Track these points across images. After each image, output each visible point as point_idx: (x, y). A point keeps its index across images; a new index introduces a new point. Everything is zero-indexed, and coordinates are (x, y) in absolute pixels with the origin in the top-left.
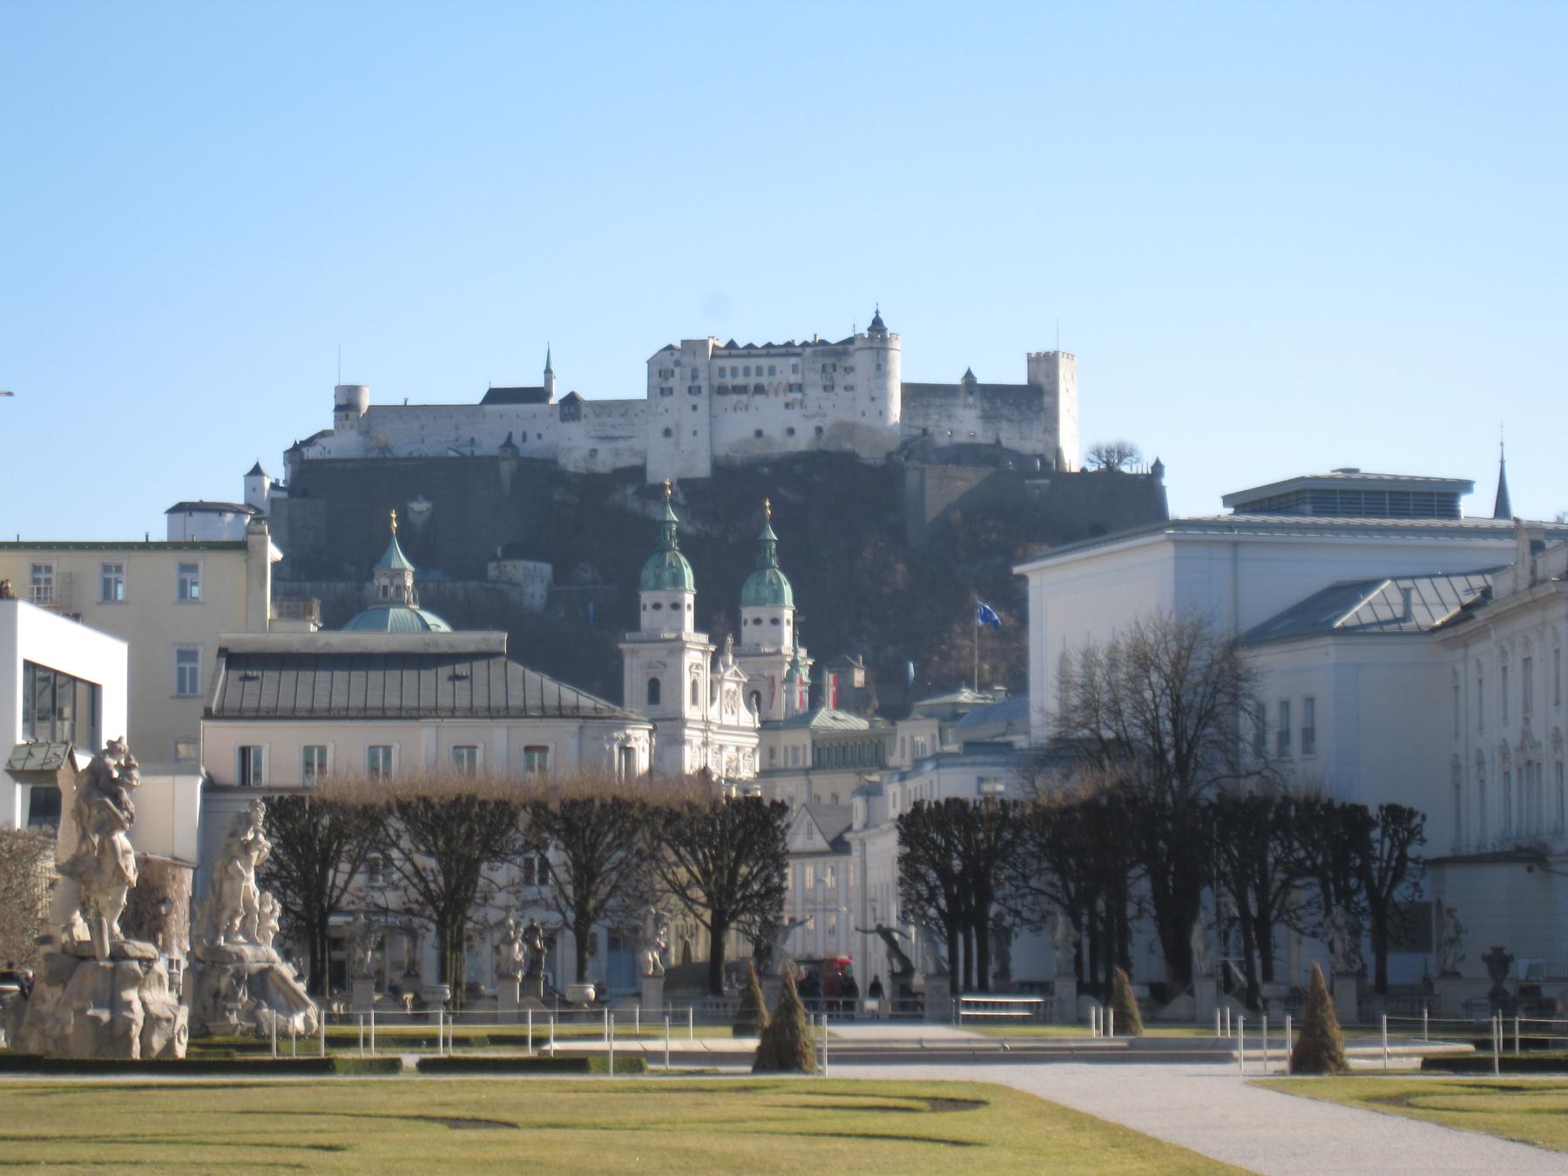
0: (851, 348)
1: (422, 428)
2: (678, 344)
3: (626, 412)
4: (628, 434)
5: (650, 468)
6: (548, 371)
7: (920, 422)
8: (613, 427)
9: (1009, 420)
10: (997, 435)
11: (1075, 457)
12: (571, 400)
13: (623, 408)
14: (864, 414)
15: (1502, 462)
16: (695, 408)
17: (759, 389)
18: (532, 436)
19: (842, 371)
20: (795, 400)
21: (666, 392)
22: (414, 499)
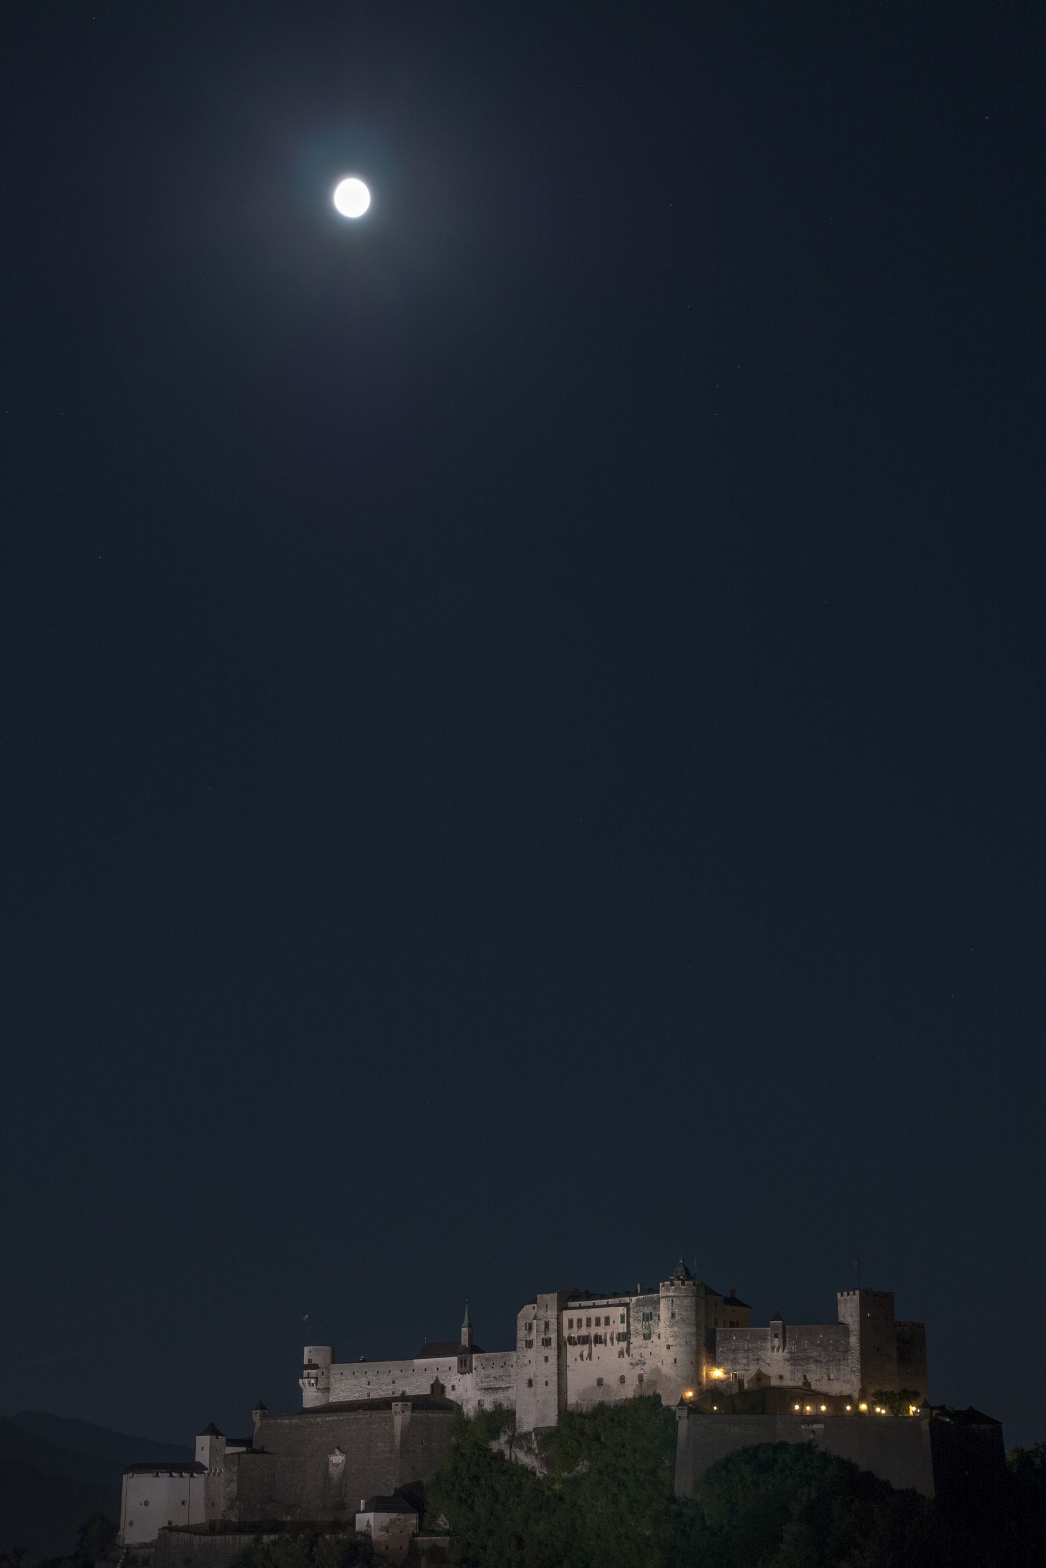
3: (505, 1363)
4: (508, 1385)
8: (495, 1378)
9: (816, 1361)
10: (805, 1377)
16: (546, 1359)
17: (598, 1340)
21: (529, 1344)
22: (333, 1453)
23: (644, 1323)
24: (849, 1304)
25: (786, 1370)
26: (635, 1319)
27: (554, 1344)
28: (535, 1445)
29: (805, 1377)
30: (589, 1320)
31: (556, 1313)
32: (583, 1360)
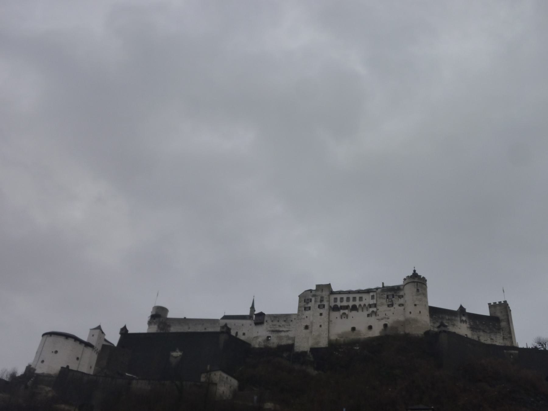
2: (314, 288)
4: (287, 330)
5: (296, 344)
6: (252, 308)
8: (280, 326)
9: (484, 331)
10: (478, 337)
12: (261, 314)
13: (286, 318)
14: (410, 313)
16: (321, 314)
17: (354, 308)
19: (397, 297)
20: (373, 312)
21: (307, 309)
22: (174, 350)
23: (388, 300)
24: (498, 308)
26: (380, 298)
27: (327, 307)
28: (311, 356)
29: (478, 337)
30: (348, 299)
31: (328, 293)
32: (341, 318)
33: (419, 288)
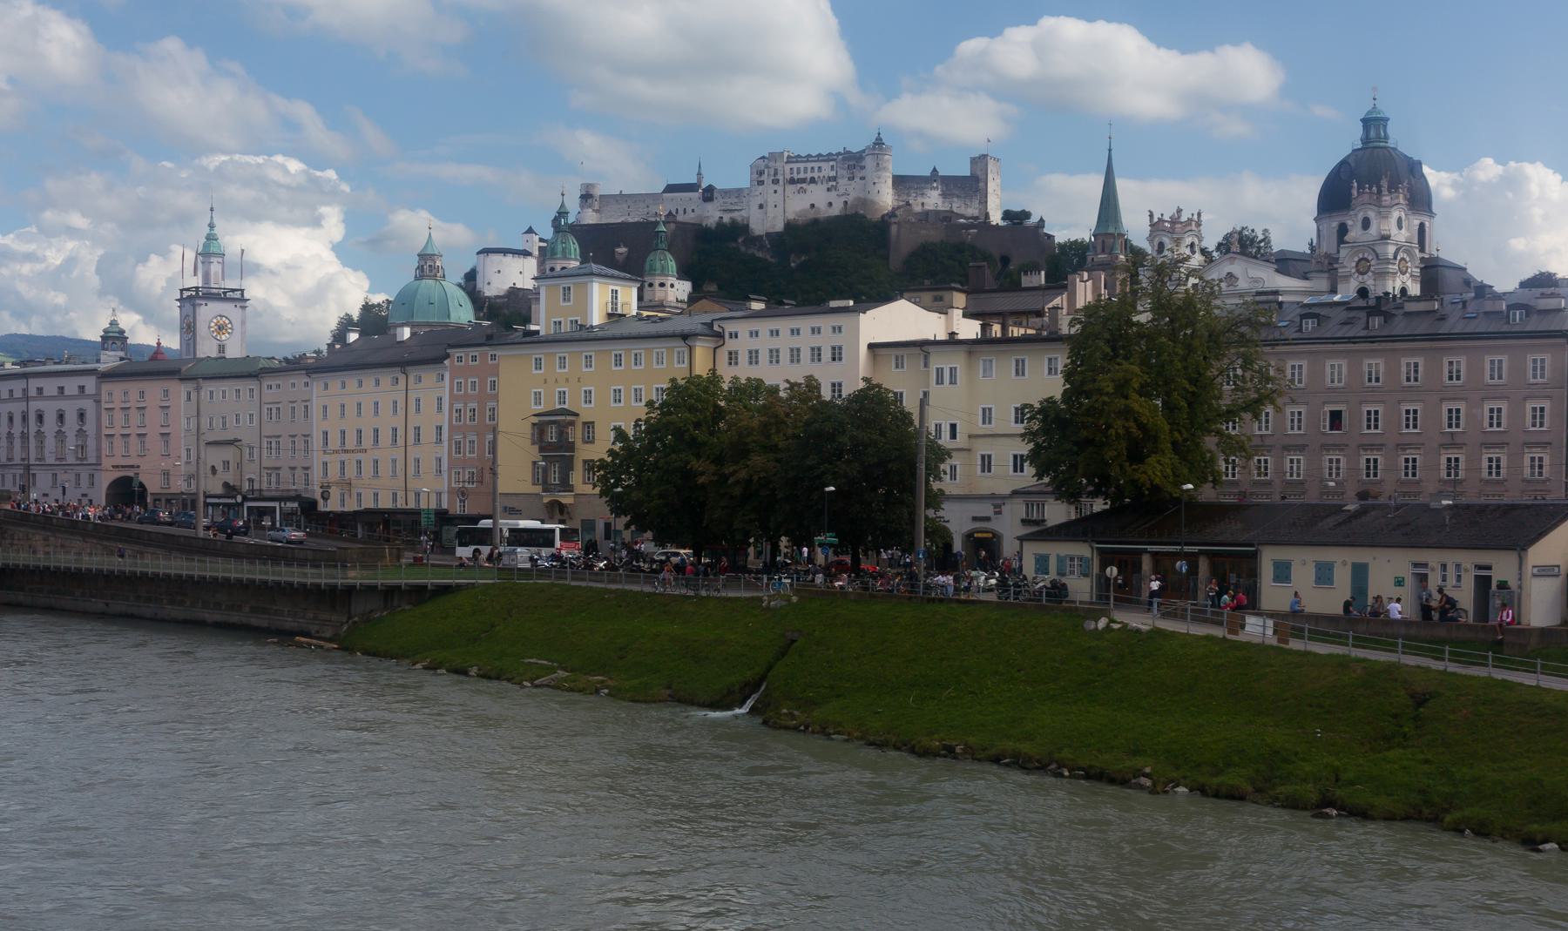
0: (864, 154)
1: (629, 207)
5: (750, 225)
6: (699, 174)
7: (905, 198)
9: (958, 197)
11: (996, 218)
12: (710, 189)
13: (739, 192)
15: (1110, 150)
16: (775, 192)
17: (813, 180)
18: (689, 210)
20: (832, 186)
21: (761, 183)
22: (619, 246)
25: (939, 201)
26: (840, 168)
28: (767, 242)
33: (880, 162)
